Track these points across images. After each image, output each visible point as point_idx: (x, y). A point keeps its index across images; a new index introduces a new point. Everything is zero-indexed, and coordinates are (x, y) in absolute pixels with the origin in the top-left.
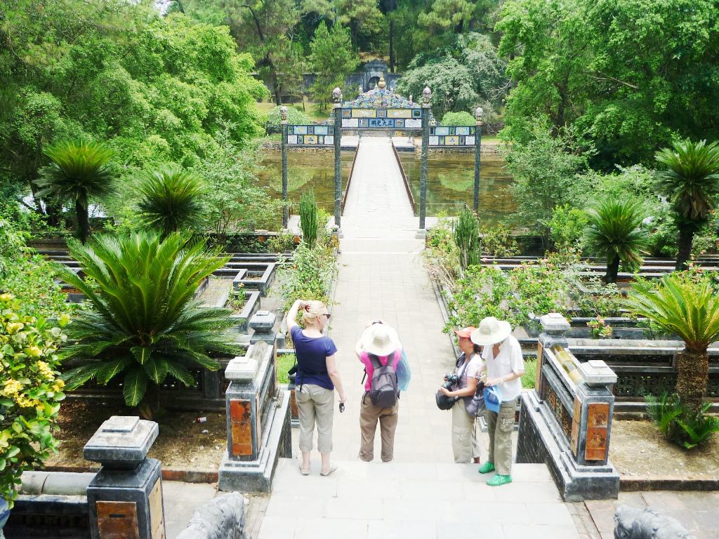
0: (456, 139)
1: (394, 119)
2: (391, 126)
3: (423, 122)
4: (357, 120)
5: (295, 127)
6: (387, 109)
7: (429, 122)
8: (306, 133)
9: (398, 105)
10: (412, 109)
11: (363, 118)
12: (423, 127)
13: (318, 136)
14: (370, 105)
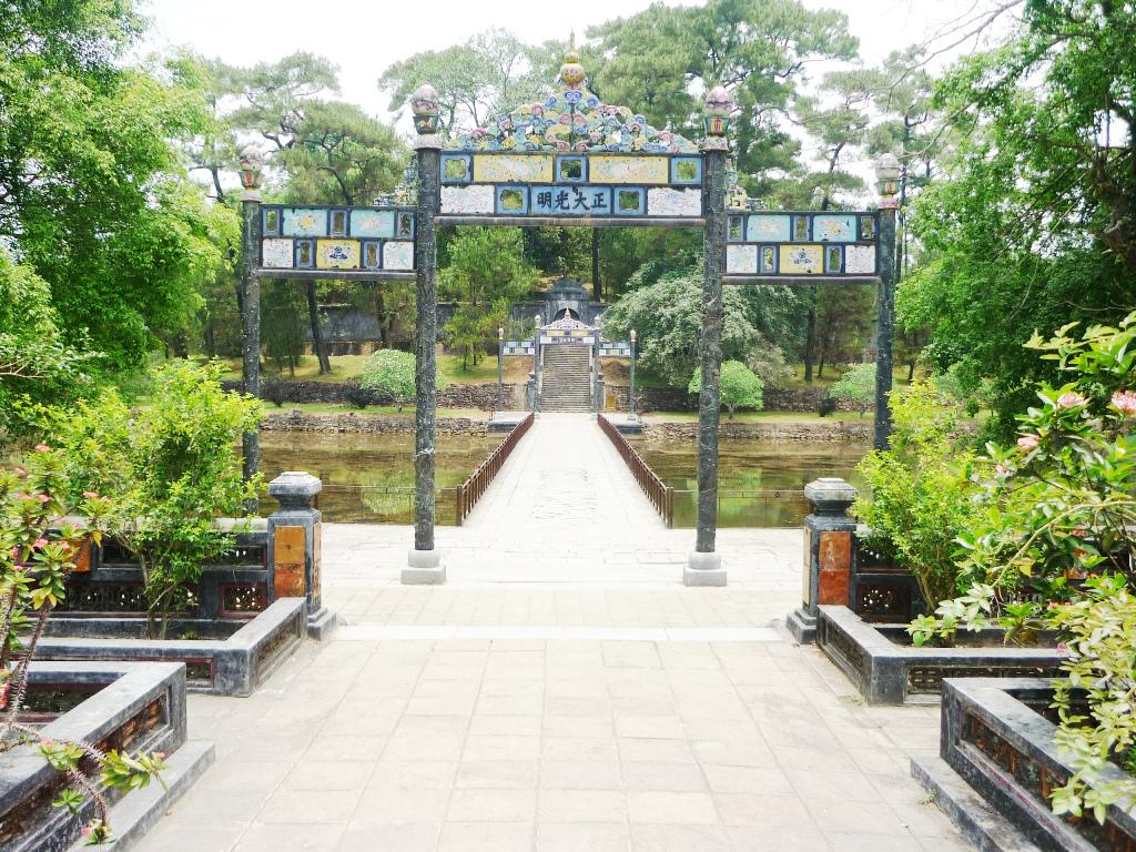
1: (612, 187)
3: (705, 199)
5: (287, 213)
6: (586, 155)
7: (727, 200)
8: (323, 233)
10: (672, 156)
11: (511, 183)
12: (706, 210)
13: (362, 240)
14: (535, 141)
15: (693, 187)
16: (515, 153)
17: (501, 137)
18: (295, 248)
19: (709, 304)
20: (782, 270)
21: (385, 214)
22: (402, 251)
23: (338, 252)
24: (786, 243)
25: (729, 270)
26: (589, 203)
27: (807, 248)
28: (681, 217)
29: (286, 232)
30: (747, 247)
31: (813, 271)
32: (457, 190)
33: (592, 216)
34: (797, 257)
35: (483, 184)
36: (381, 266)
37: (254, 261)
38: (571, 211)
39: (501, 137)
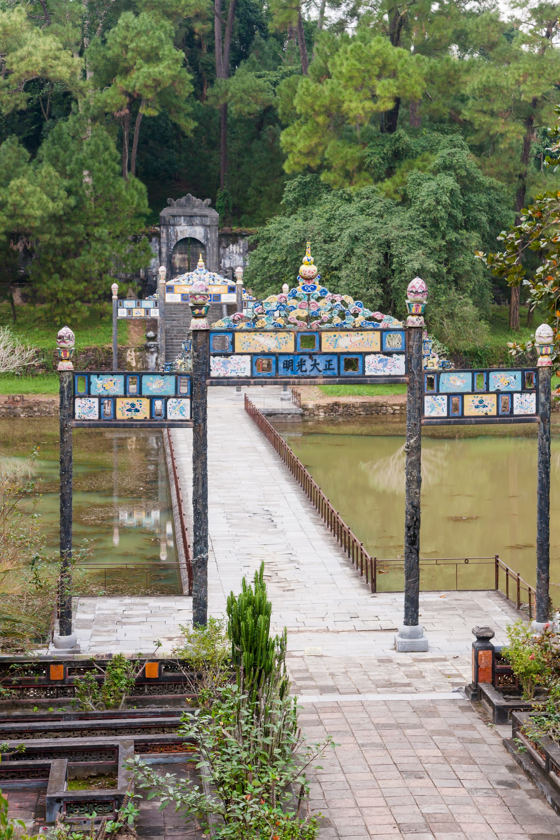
0: (490, 400)
2: (329, 373)
4: (248, 358)
6: (319, 332)
9: (350, 321)
11: (263, 354)
12: (408, 370)
13: (152, 398)
15: (398, 353)
16: (266, 331)
17: (256, 319)
18: (100, 404)
19: (412, 441)
20: (466, 414)
21: (168, 377)
22: (181, 405)
23: (133, 408)
24: (468, 393)
25: (427, 414)
26: (321, 367)
27: (484, 397)
28: (390, 376)
29: (93, 393)
30: (439, 397)
31: (489, 414)
32: (223, 359)
33: (324, 377)
34: (477, 403)
35: (242, 354)
36: (166, 417)
37: (69, 415)
38: (308, 373)
39: (256, 319)
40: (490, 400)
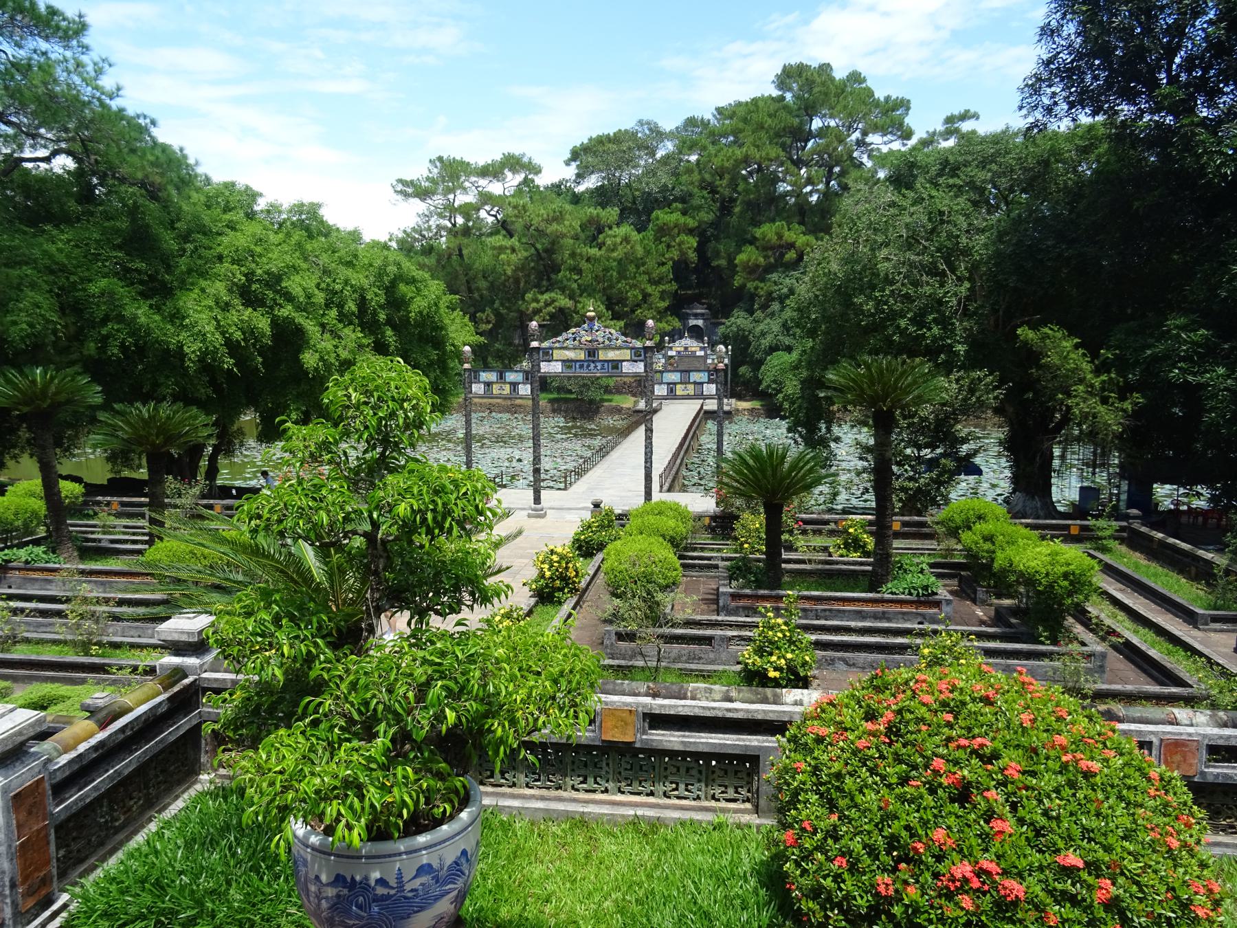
3: (645, 366)
6: (598, 349)
10: (632, 349)
12: (646, 371)
40: (691, 387)
